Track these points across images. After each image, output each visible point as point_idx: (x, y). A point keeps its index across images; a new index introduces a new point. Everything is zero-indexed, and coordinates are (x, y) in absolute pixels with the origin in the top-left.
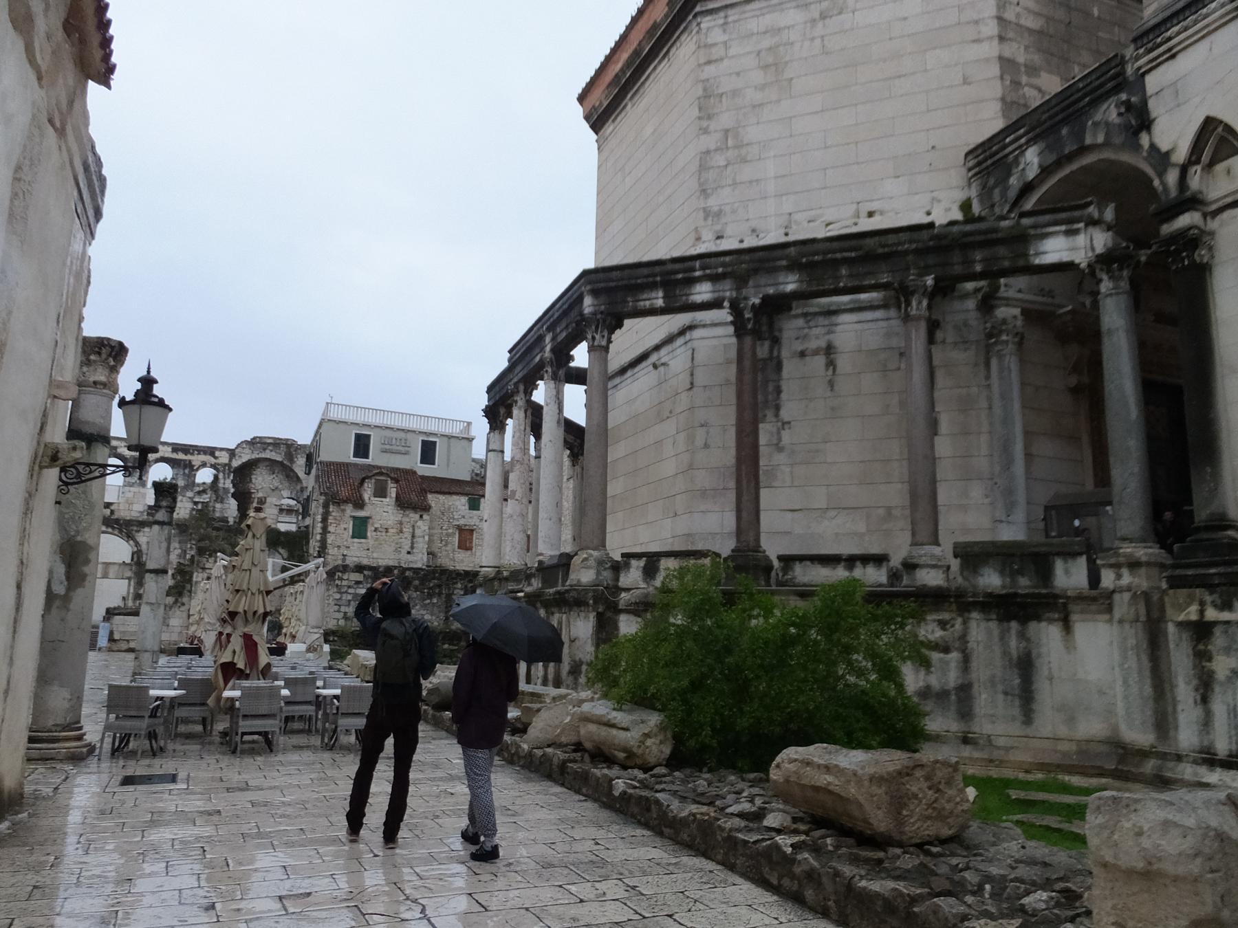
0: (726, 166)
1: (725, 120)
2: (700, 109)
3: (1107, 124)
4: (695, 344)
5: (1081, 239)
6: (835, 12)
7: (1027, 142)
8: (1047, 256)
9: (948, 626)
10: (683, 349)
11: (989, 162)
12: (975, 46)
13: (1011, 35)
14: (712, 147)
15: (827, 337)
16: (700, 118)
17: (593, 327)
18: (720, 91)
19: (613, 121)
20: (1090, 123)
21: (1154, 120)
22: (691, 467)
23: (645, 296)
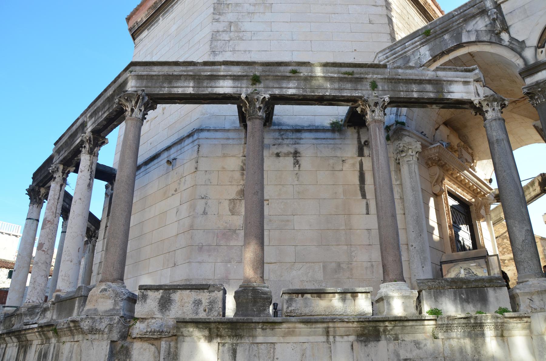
0: (229, 41)
1: (230, 17)
2: (214, 9)
3: (477, 31)
4: (201, 142)
5: (472, 88)
7: (420, 44)
8: (454, 93)
10: (191, 145)
11: (394, 56)
12: (375, 7)
14: (221, 29)
15: (294, 146)
16: (214, 14)
17: (133, 103)
18: (228, 2)
19: (148, 30)
20: (464, 31)
22: (191, 227)
23: (179, 84)
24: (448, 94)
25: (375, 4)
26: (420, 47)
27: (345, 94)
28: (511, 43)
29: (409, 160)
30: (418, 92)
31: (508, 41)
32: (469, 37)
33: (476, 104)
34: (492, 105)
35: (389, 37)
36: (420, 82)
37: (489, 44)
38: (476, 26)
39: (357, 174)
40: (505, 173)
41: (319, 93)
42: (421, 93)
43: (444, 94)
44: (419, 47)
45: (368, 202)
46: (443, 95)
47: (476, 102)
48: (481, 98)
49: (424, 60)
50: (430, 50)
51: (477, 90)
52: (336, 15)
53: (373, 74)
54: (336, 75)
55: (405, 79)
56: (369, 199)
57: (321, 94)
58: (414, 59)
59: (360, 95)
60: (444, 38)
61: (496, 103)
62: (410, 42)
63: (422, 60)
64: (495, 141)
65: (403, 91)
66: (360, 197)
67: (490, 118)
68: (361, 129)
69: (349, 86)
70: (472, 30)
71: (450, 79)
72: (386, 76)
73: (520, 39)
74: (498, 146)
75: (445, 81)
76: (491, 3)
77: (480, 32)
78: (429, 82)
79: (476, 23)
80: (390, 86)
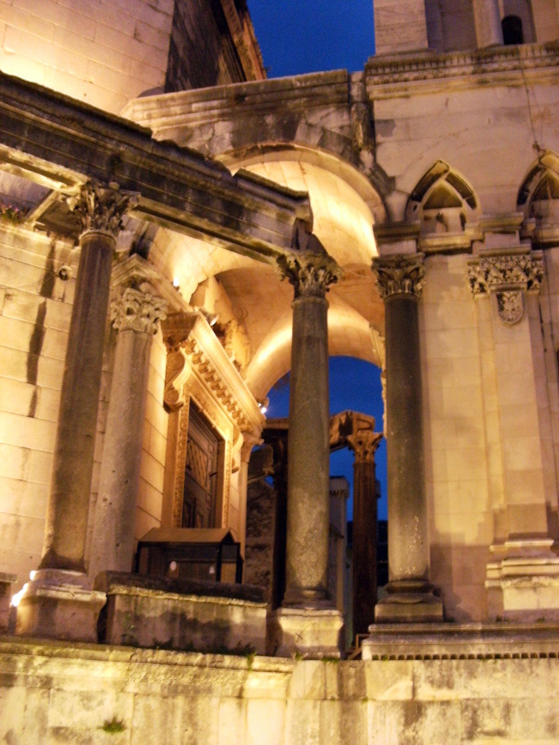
3: (324, 130)
9: (94, 703)
13: (179, 25)
20: (303, 121)
21: (380, 144)
25: (154, 6)
26: (218, 121)
28: (373, 173)
31: (370, 169)
38: (325, 120)
39: (28, 331)
40: (308, 402)
44: (216, 119)
45: (38, 392)
50: (233, 132)
56: (40, 388)
58: (200, 139)
60: (264, 121)
62: (201, 105)
63: (215, 146)
66: (24, 378)
70: (316, 124)
73: (390, 173)
77: (328, 135)
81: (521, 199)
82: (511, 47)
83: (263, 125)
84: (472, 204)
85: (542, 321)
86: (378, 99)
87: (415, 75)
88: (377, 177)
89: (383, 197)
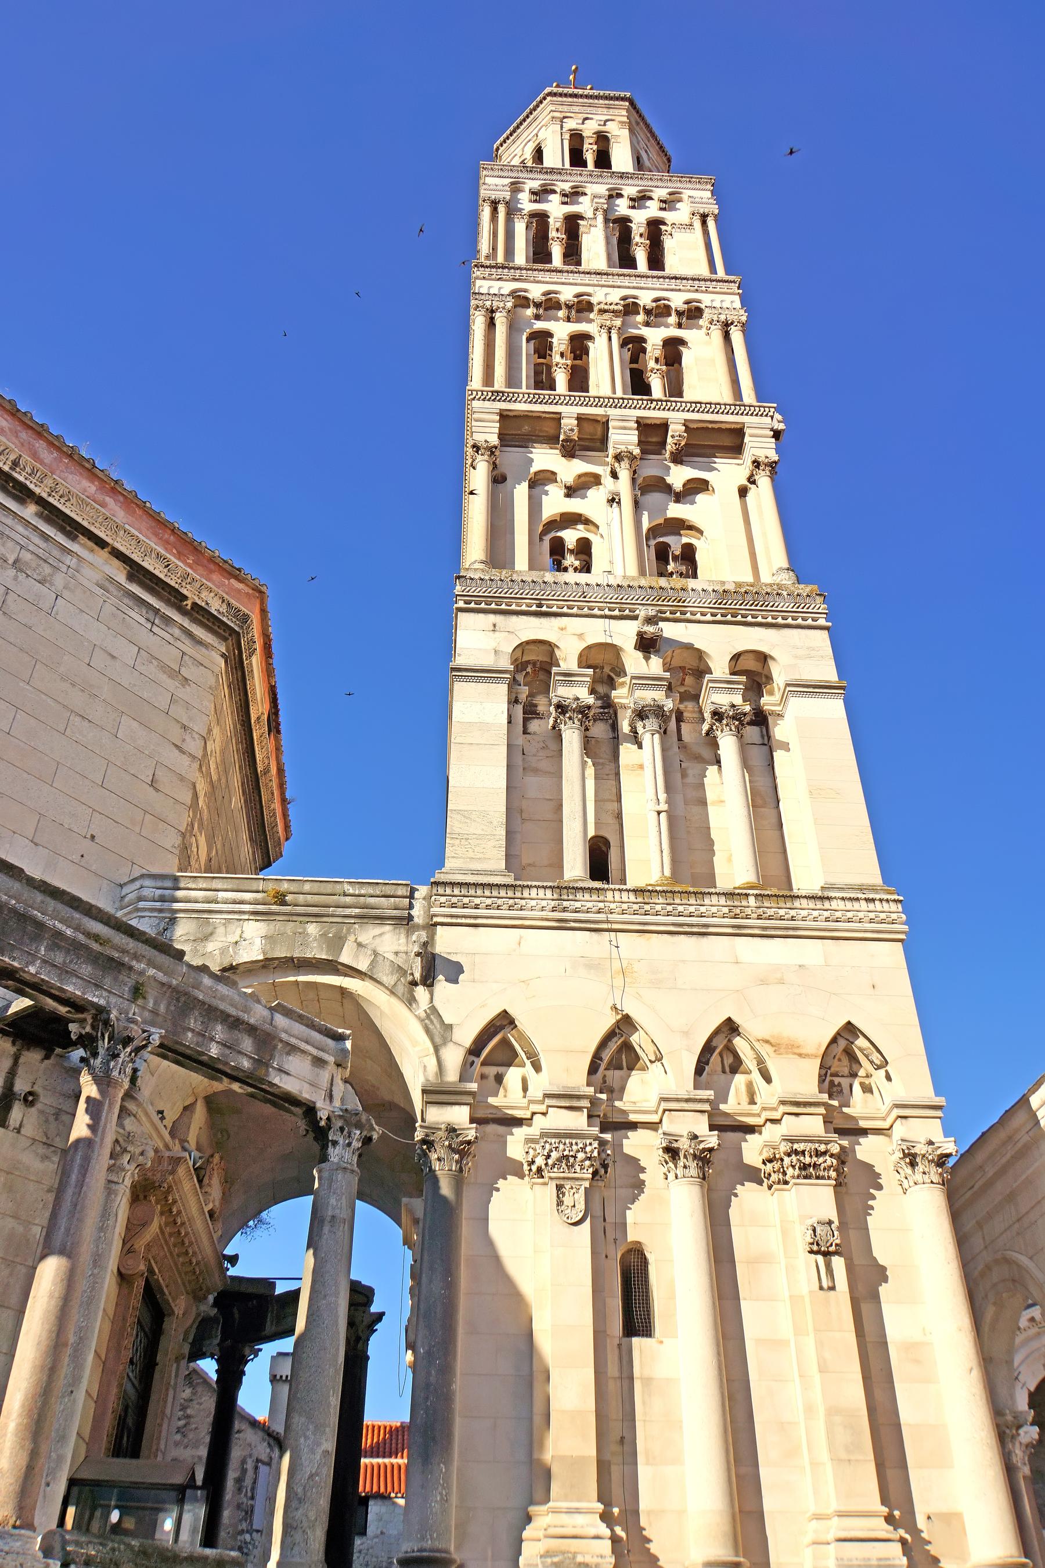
3: (374, 951)
5: (325, 1076)
6: (35, 577)
13: (204, 769)
20: (352, 938)
24: (278, 1073)
27: (70, 988)
28: (428, 1016)
29: (116, 1180)
30: (225, 1045)
31: (425, 1011)
32: (356, 956)
33: (321, 1119)
34: (349, 1134)
35: (178, 841)
36: (235, 1024)
37: (388, 993)
38: (378, 940)
40: (324, 1302)
41: (14, 959)
42: (228, 1052)
43: (271, 1069)
46: (267, 1074)
47: (323, 1115)
48: (336, 1110)
49: (245, 955)
51: (332, 1085)
52: (86, 723)
53: (151, 963)
54: (69, 932)
55: (209, 1005)
57: (16, 964)
59: (102, 1002)
60: (305, 929)
61: (358, 1132)
64: (328, 1219)
65: (193, 1031)
67: (336, 1160)
68: (28, 1050)
69: (86, 970)
71: (293, 1041)
72: (174, 982)
74: (330, 1231)
75: (281, 1041)
76: (422, 912)
77: (380, 959)
78: (252, 1030)
79: (381, 935)
80: (173, 1008)
81: (593, 1069)
82: (597, 884)
83: (304, 934)
84: (537, 1067)
85: (605, 1220)
86: (443, 924)
87: (489, 901)
88: (432, 1022)
89: (437, 1049)
